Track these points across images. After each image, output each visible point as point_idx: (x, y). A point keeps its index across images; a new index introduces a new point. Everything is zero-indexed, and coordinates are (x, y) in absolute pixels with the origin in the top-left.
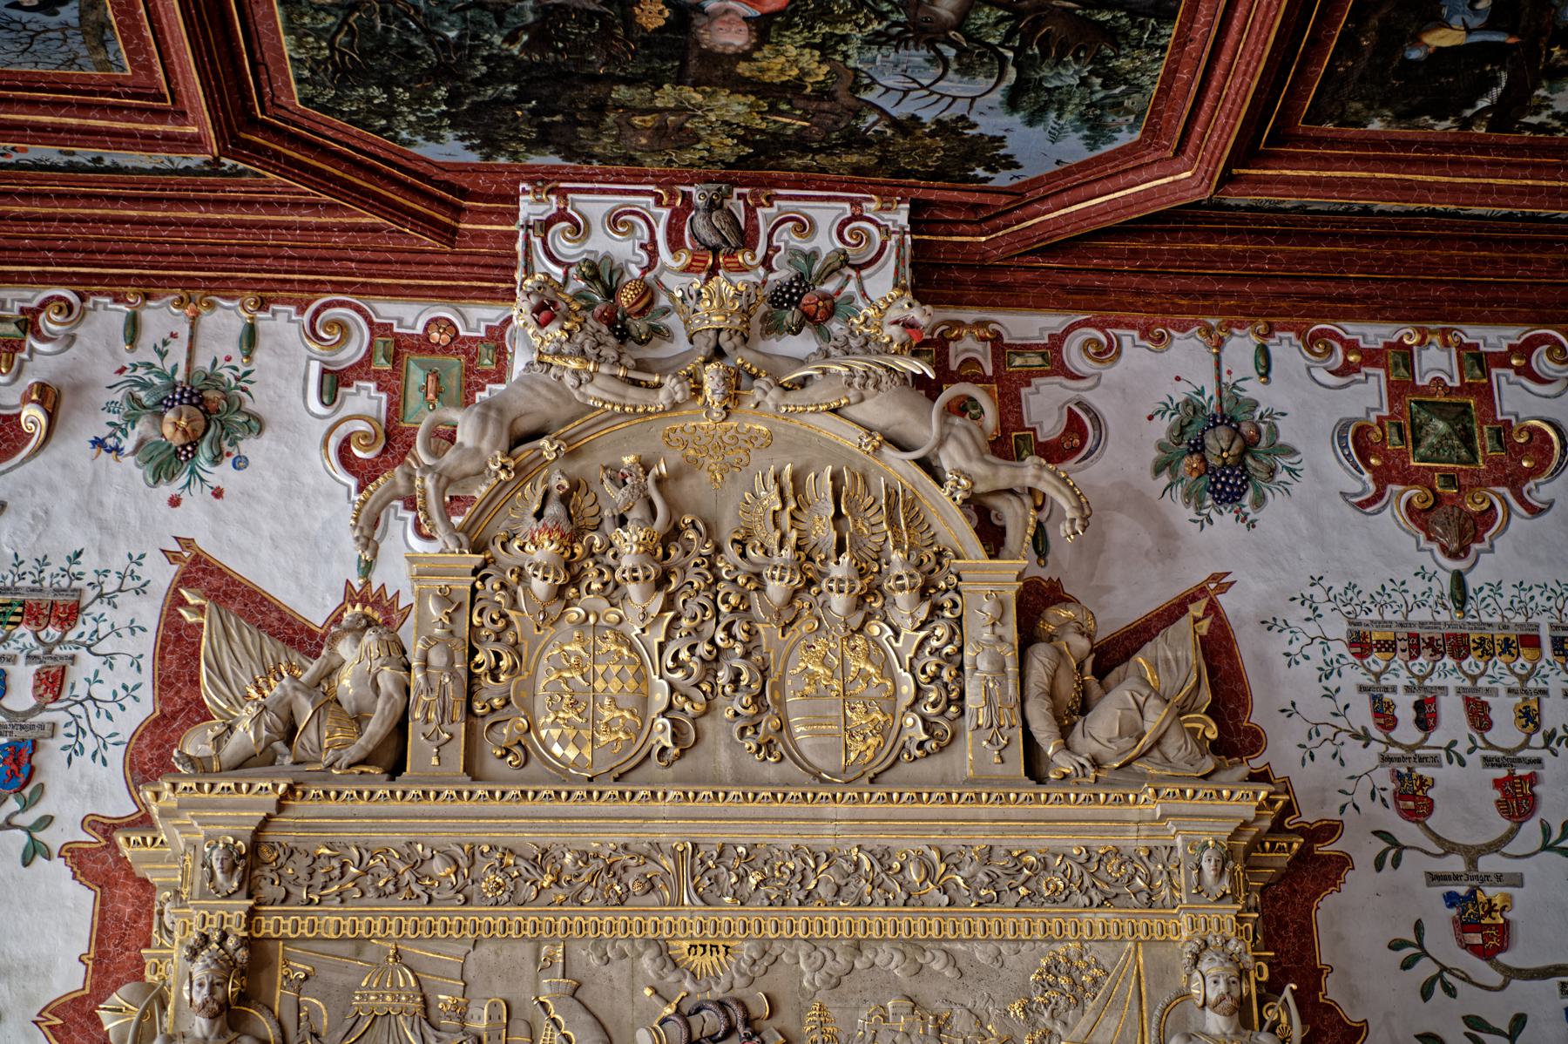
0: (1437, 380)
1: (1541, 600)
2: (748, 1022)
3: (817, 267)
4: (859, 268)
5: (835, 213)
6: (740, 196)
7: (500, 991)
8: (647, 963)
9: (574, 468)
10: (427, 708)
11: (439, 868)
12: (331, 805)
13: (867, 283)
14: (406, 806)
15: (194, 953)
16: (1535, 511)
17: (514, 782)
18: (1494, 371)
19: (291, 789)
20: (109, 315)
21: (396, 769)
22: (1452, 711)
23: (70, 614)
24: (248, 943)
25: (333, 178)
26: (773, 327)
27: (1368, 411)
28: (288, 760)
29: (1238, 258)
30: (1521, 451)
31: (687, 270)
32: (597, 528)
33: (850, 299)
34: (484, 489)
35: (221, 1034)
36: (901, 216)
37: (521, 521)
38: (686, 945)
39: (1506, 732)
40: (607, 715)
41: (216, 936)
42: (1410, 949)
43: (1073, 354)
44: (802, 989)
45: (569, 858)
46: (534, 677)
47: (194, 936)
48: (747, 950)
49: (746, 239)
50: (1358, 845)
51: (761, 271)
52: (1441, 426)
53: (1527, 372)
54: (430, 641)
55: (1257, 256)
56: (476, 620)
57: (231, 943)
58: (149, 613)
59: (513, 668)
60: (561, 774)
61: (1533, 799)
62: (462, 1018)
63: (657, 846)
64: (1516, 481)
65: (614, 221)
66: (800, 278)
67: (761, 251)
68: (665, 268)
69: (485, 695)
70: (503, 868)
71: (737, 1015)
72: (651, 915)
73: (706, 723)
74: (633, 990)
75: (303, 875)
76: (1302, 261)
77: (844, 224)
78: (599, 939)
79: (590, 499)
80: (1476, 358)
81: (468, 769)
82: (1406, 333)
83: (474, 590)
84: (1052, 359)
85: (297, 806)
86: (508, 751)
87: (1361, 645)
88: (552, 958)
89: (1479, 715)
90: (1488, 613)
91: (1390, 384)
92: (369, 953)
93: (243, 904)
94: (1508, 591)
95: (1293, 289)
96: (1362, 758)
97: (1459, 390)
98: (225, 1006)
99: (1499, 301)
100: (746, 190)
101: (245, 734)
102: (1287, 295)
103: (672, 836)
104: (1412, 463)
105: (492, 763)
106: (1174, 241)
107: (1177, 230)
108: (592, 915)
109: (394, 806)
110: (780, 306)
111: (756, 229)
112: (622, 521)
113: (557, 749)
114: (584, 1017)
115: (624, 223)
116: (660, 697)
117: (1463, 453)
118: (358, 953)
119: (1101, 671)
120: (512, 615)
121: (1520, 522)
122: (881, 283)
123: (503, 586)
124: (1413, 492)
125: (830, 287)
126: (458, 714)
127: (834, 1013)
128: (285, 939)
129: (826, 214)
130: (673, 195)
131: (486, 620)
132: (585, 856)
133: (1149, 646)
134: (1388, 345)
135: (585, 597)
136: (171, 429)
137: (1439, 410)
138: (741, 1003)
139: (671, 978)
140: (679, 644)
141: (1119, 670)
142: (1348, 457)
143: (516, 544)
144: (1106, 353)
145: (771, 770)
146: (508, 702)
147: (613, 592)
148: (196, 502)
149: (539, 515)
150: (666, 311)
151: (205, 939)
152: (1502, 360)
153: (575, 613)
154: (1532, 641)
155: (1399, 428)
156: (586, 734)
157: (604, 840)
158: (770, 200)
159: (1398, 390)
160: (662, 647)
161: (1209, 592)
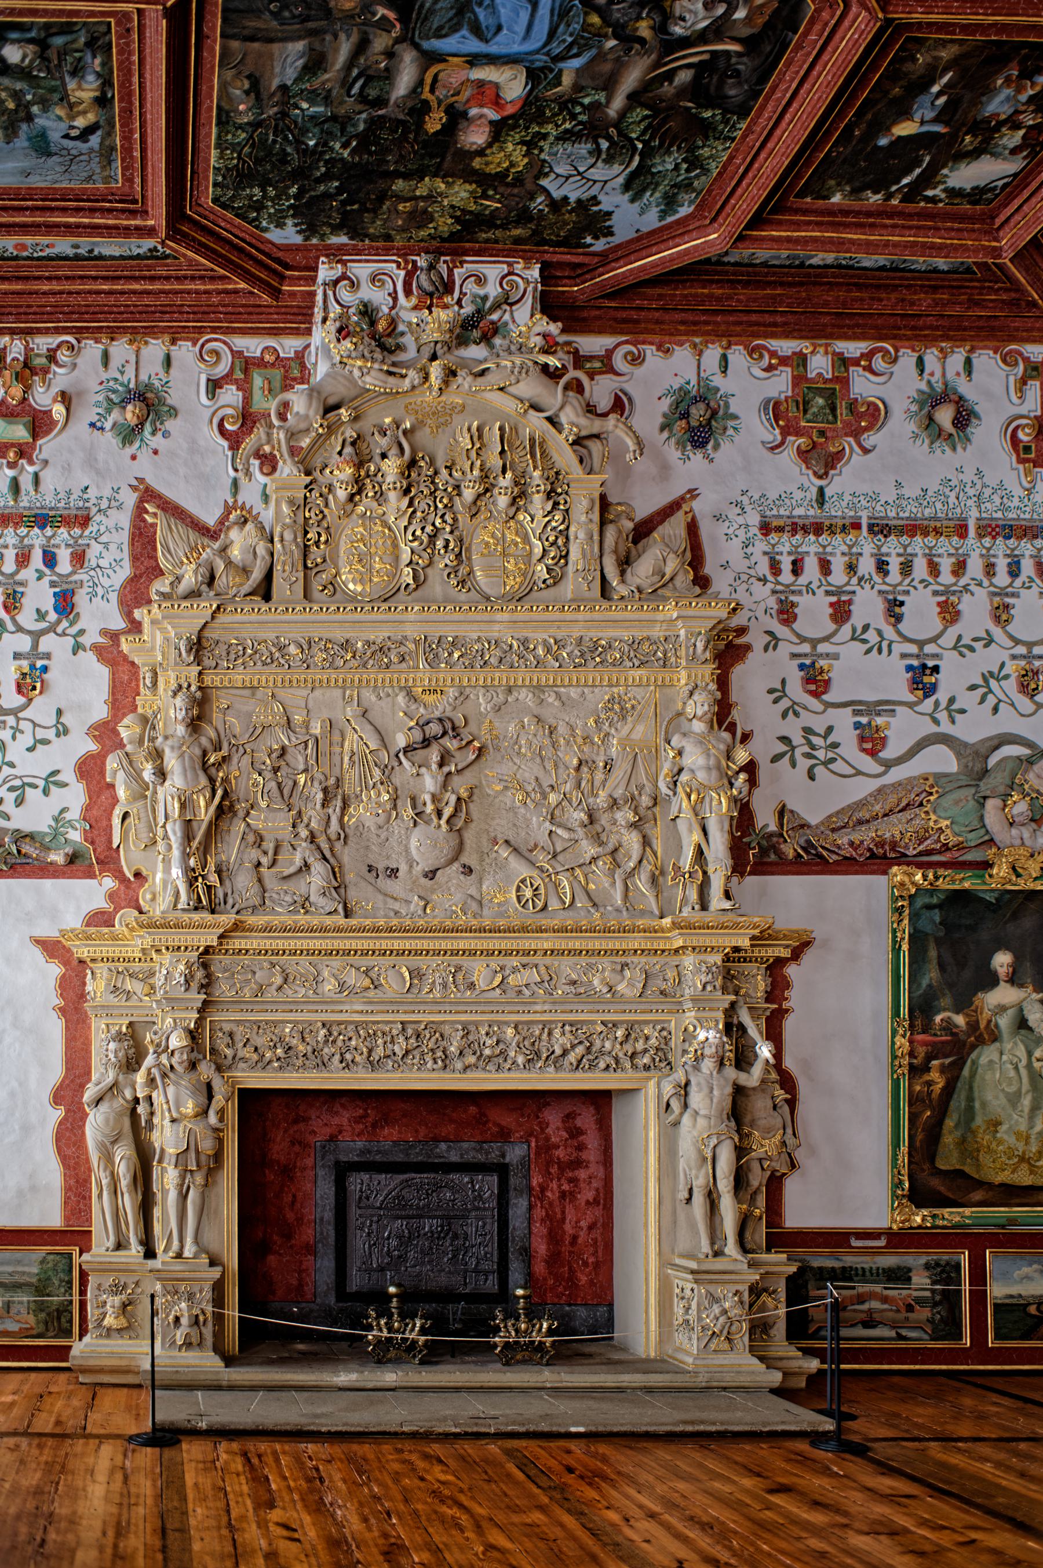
0: (820, 374)
1: (864, 503)
2: (454, 729)
3: (488, 305)
4: (511, 305)
5: (497, 271)
6: (445, 262)
7: (326, 714)
8: (401, 699)
9: (357, 426)
10: (284, 564)
11: (293, 649)
12: (238, 617)
13: (516, 314)
14: (278, 617)
15: (175, 694)
16: (866, 451)
17: (333, 602)
18: (851, 369)
19: (218, 607)
21: (267, 597)
24: (200, 688)
25: (221, 256)
26: (462, 341)
27: (780, 393)
28: (212, 593)
29: (719, 299)
30: (861, 416)
31: (415, 308)
32: (370, 461)
33: (506, 324)
34: (308, 441)
35: (191, 735)
36: (535, 273)
37: (330, 457)
38: (420, 690)
40: (377, 566)
41: (185, 685)
44: (481, 713)
45: (360, 645)
46: (337, 546)
47: (174, 686)
48: (452, 692)
49: (448, 287)
51: (456, 308)
52: (821, 401)
53: (869, 369)
54: (285, 526)
55: (729, 298)
56: (307, 515)
57: (193, 688)
59: (327, 542)
60: (353, 598)
61: (849, 613)
62: (307, 728)
63: (405, 638)
64: (856, 433)
65: (374, 279)
66: (478, 311)
67: (456, 295)
68: (401, 307)
69: (312, 557)
70: (326, 650)
71: (448, 725)
72: (402, 674)
73: (429, 571)
74: (394, 714)
75: (224, 654)
76: (755, 300)
77: (503, 278)
78: (376, 687)
79: (365, 445)
80: (843, 362)
81: (305, 597)
83: (306, 498)
85: (222, 618)
86: (325, 587)
88: (351, 697)
90: (836, 510)
91: (794, 377)
92: (259, 694)
93: (195, 669)
94: (847, 498)
95: (745, 319)
97: (831, 380)
98: (193, 720)
99: (858, 326)
100: (448, 258)
101: (190, 578)
102: (740, 323)
103: (412, 631)
104: (803, 424)
105: (316, 595)
106: (685, 288)
107: (686, 281)
108: (372, 674)
109: (270, 617)
110: (467, 329)
111: (454, 282)
112: (384, 456)
113: (351, 586)
114: (369, 727)
115: (379, 280)
116: (406, 556)
117: (830, 417)
118: (253, 694)
119: (635, 542)
120: (326, 511)
121: (857, 459)
122: (523, 313)
123: (321, 495)
124: (801, 440)
125: (495, 317)
126: (301, 567)
127: (497, 724)
128: (217, 688)
129: (493, 271)
130: (407, 262)
131: (313, 515)
132: (368, 643)
133: (660, 528)
134: (794, 353)
135: (365, 500)
137: (819, 392)
138: (450, 719)
139: (414, 707)
140: (416, 526)
141: (645, 541)
142: (769, 420)
143: (328, 471)
145: (463, 596)
146: (324, 561)
147: (380, 497)
149: (340, 453)
150: (402, 334)
151: (180, 687)
152: (856, 362)
153: (361, 509)
154: (857, 526)
155: (797, 402)
156: (366, 578)
157: (379, 635)
158: (462, 263)
159: (798, 380)
160: (406, 528)
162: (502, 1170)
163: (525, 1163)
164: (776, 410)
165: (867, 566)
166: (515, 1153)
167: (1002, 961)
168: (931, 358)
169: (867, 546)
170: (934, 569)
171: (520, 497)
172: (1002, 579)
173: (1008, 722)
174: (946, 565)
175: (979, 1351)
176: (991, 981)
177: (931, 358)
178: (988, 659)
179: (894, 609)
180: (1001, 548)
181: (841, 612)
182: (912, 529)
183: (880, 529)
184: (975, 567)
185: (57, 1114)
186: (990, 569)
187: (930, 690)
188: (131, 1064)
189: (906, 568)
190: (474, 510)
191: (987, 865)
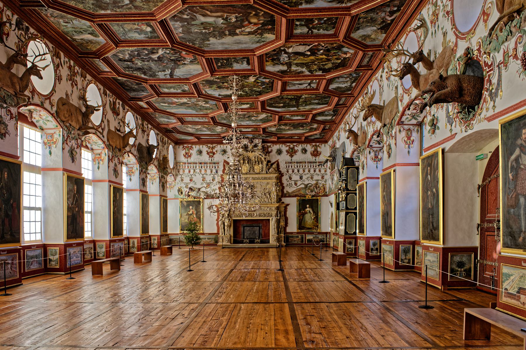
20: (219, 146)
22: (290, 167)
23: (219, 163)
39: (293, 168)
42: (287, 180)
43: (271, 146)
50: (285, 174)
58: (222, 163)
80: (294, 146)
82: (290, 144)
84: (270, 146)
87: (286, 163)
89: (292, 167)
90: (293, 161)
96: (285, 170)
136: (223, 153)
144: (273, 146)
148: (224, 157)
159: (289, 148)
161: (277, 161)
162: (259, 227)
163: (262, 226)
164: (287, 151)
165: (296, 166)
166: (261, 225)
167: (308, 206)
168: (303, 145)
169: (296, 164)
170: (303, 167)
171: (259, 163)
172: (309, 167)
173: (310, 182)
174: (304, 166)
175: (305, 244)
176: (307, 208)
177: (303, 145)
178: (308, 176)
179: (298, 171)
180: (309, 164)
181: (293, 171)
182: (300, 163)
183: (297, 163)
184: (307, 166)
185: (217, 222)
186: (308, 167)
187: (302, 179)
188: (223, 217)
189: (300, 167)
190: (255, 164)
191: (306, 197)
